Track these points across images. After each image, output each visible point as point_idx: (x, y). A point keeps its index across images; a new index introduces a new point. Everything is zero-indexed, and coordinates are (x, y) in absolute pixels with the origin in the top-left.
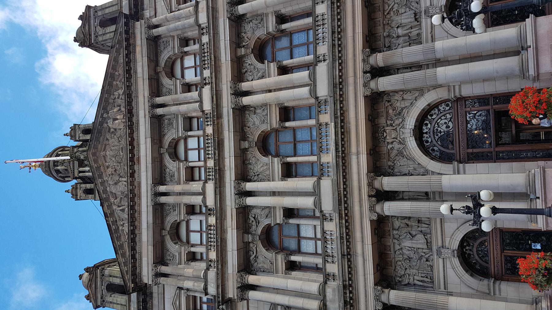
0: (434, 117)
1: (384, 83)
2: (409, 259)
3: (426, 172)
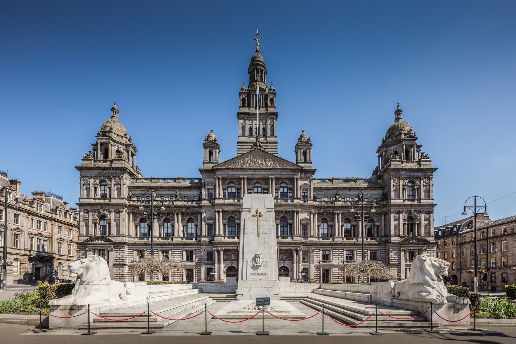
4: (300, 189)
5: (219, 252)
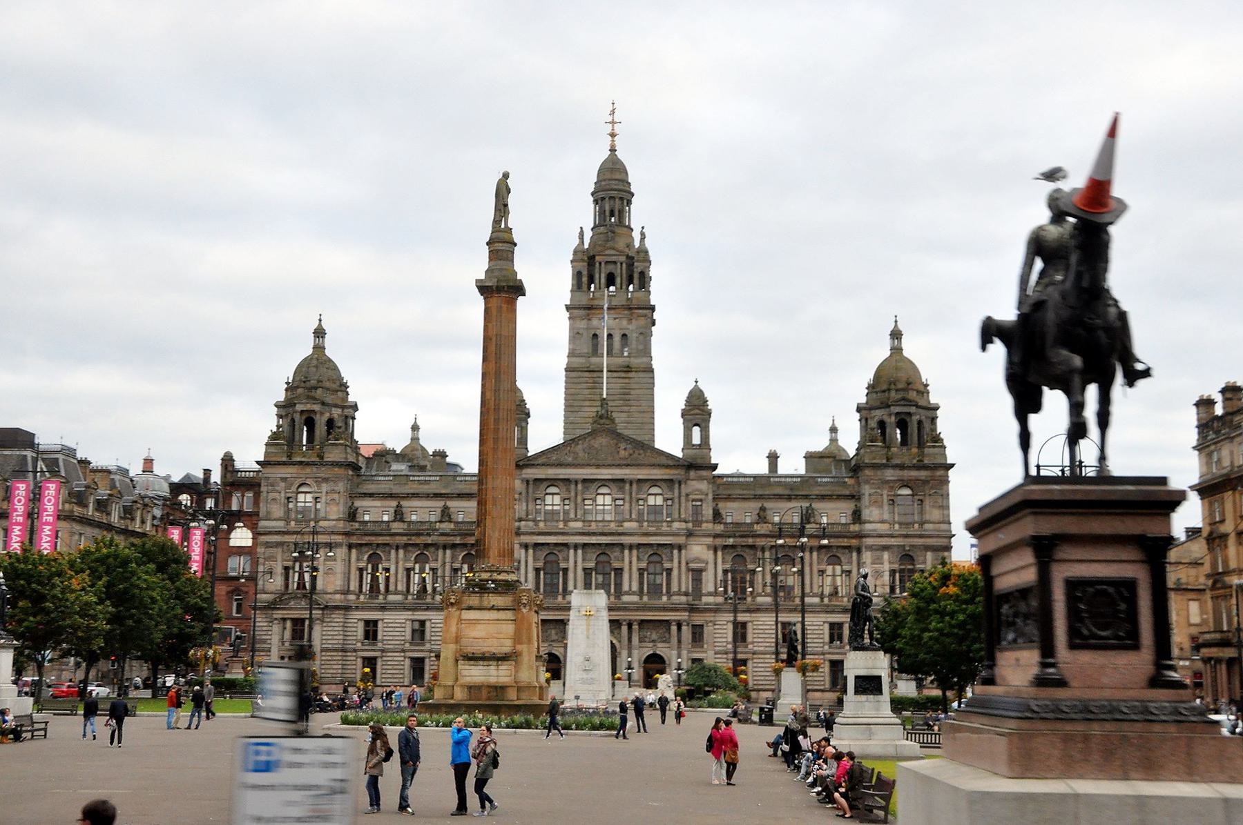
4: (687, 500)
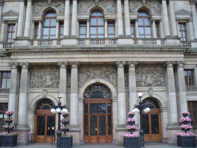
0: (105, 91)
1: (121, 71)
2: (42, 78)
3: (79, 86)
5: (19, 68)
